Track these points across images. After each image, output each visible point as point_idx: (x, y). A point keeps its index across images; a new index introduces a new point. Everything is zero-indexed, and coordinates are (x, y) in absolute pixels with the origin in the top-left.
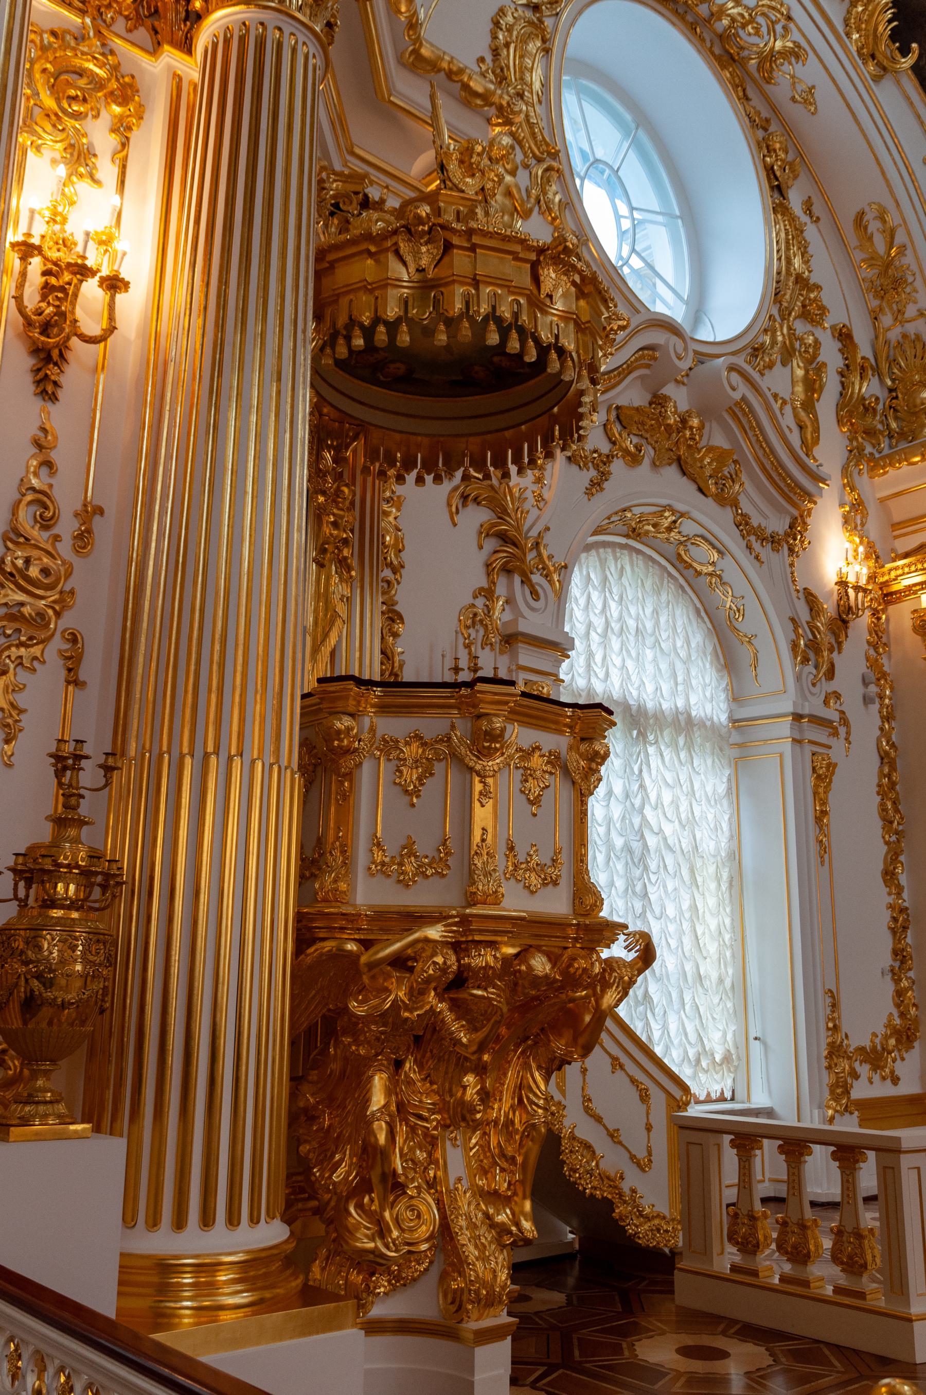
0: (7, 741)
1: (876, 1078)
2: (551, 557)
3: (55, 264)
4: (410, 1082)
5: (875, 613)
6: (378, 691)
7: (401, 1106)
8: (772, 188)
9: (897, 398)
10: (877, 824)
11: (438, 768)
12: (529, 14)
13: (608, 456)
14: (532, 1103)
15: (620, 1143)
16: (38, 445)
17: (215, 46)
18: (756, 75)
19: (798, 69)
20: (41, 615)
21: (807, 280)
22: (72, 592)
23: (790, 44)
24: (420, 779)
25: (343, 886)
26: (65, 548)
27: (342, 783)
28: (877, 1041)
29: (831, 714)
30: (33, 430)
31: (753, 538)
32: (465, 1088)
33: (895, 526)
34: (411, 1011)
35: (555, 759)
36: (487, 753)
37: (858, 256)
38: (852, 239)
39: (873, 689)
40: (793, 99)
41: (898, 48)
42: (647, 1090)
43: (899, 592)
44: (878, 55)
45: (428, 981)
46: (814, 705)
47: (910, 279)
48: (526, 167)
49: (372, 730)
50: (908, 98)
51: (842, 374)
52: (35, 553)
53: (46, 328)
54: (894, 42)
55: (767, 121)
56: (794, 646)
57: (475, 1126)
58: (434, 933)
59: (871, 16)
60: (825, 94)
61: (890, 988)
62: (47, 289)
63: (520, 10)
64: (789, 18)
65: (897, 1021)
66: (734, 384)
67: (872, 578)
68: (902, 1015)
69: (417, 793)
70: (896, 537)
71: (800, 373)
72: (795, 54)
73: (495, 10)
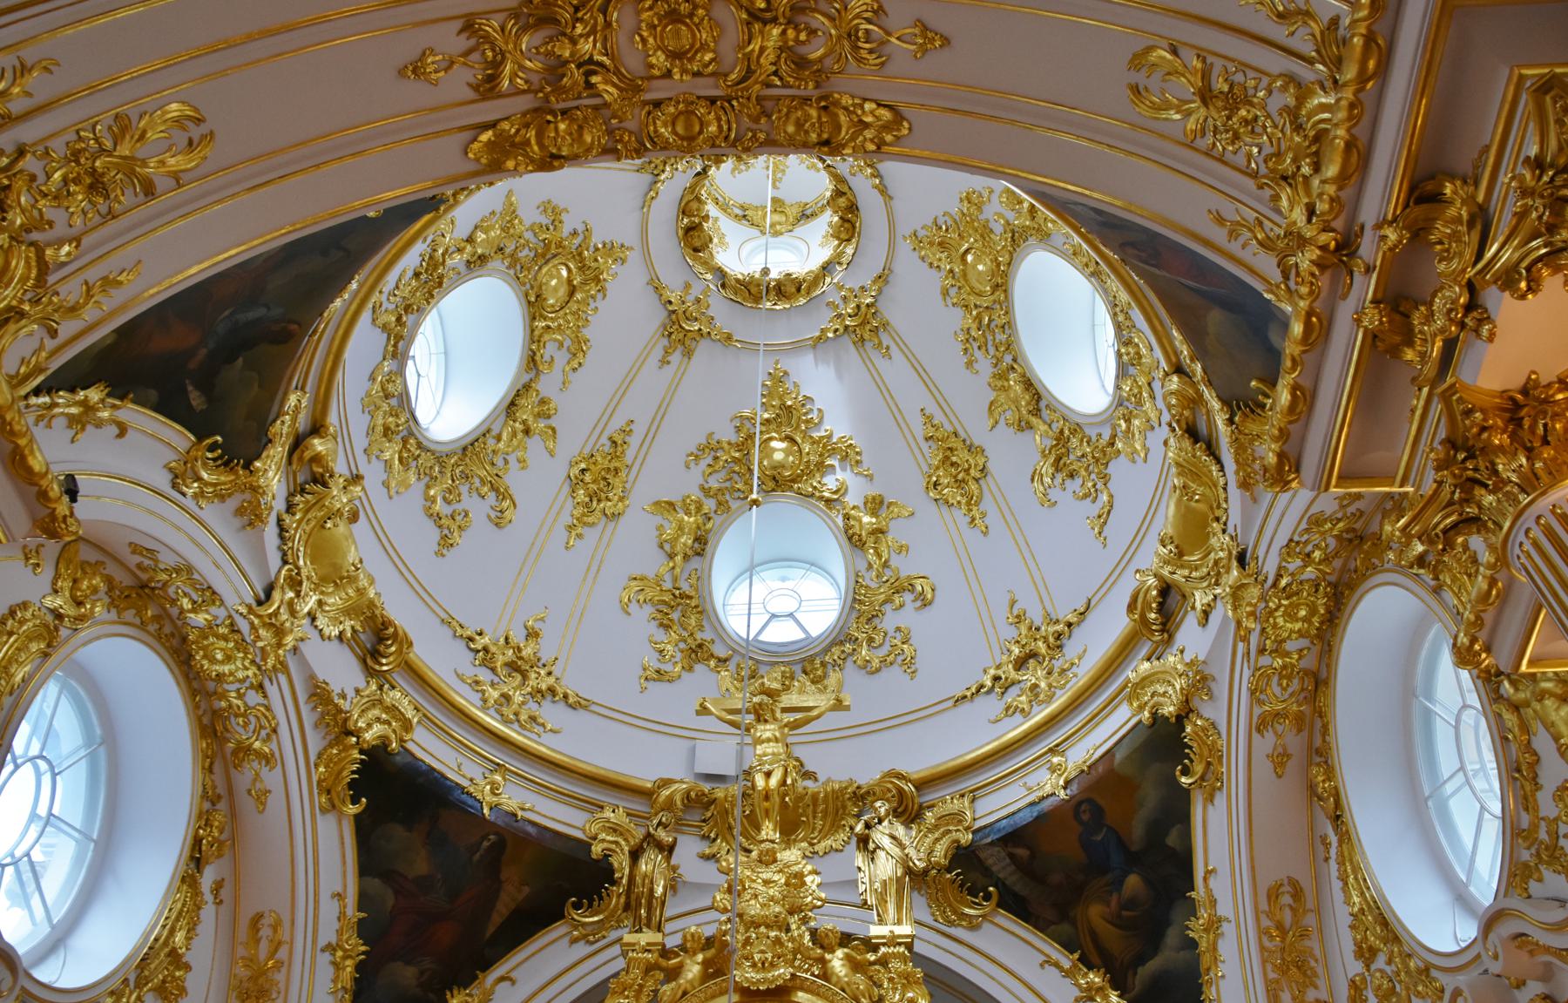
8: (192, 858)
12: (49, 618)
18: (229, 756)
19: (265, 771)
21: (180, 956)
23: (267, 750)
37: (241, 951)
40: (249, 792)
41: (351, 796)
44: (333, 793)
47: (274, 996)
50: (342, 838)
54: (350, 789)
55: (219, 797)
59: (340, 760)
60: (275, 801)
63: (44, 610)
64: (275, 731)
72: (267, 759)
73: (19, 601)
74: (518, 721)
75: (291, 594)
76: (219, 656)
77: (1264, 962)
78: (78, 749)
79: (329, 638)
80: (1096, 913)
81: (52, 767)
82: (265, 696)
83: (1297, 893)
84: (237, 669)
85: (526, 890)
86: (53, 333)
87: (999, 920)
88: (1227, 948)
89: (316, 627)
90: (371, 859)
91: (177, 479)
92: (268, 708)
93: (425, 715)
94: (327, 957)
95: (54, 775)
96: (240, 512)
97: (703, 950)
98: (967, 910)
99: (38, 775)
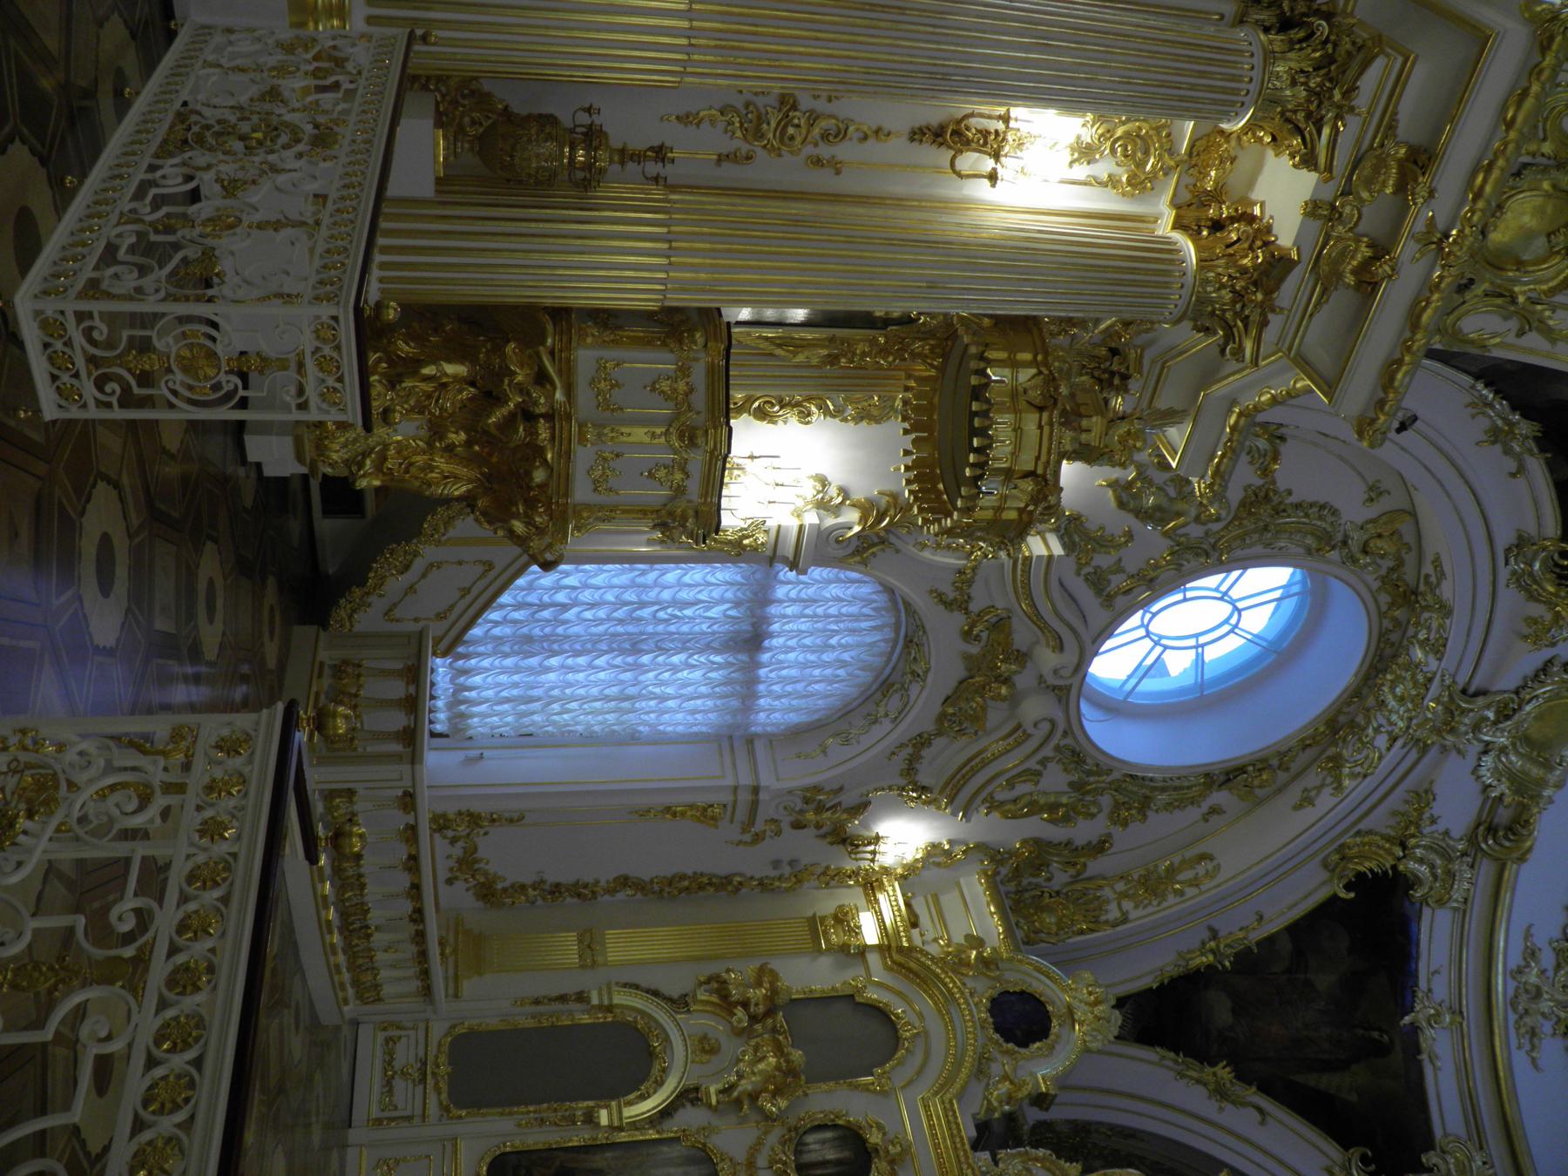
0: (678, 118)
1: (452, 863)
2: (874, 554)
3: (1004, 139)
4: (460, 391)
5: (855, 874)
6: (723, 363)
7: (444, 385)
8: (1227, 774)
9: (1051, 896)
10: (668, 871)
11: (672, 404)
12: (1339, 537)
13: (966, 609)
14: (446, 485)
15: (406, 594)
16: (878, 131)
17: (1169, 243)
20: (762, 136)
22: (780, 155)
24: (663, 392)
25: (589, 340)
26: (809, 150)
27: (659, 339)
28: (482, 865)
29: (759, 826)
30: (887, 126)
31: (910, 750)
32: (457, 433)
33: (936, 898)
34: (509, 385)
35: (680, 491)
36: (681, 437)
38: (1190, 853)
39: (787, 870)
42: (445, 618)
43: (875, 896)
45: (529, 394)
46: (766, 811)
48: (1207, 533)
49: (696, 360)
51: (1068, 843)
52: (804, 131)
53: (956, 133)
55: (1288, 769)
56: (817, 789)
57: (430, 444)
58: (559, 395)
61: (527, 879)
62: (985, 133)
64: (1365, 776)
65: (499, 886)
66: (1040, 726)
67: (886, 871)
68: (505, 890)
69: (653, 389)
71: (1064, 800)
73: (1337, 506)
74: (1521, 1017)
75: (1491, 715)
76: (1398, 691)
78: (1266, 640)
79: (1479, 777)
81: (1236, 626)
82: (1389, 749)
84: (1397, 712)
85: (1354, 1098)
86: (1521, 333)
89: (1480, 759)
90: (1305, 930)
91: (1521, 544)
92: (1380, 758)
93: (1465, 911)
94: (1206, 934)
95: (1232, 631)
96: (1532, 621)
99: (1226, 621)
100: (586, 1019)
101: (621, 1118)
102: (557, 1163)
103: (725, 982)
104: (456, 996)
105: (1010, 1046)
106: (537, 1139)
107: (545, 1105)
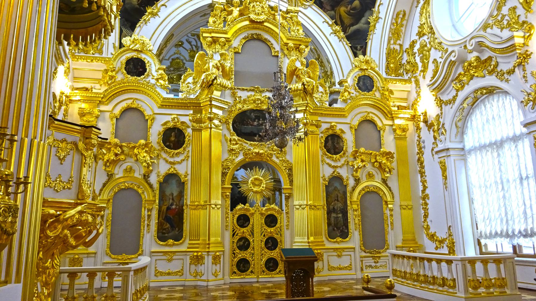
70: (74, 82)
77: (390, 32)
80: (342, 10)
83: (404, 15)
87: (313, 7)
88: (379, 26)
97: (239, 6)
98: (304, 3)
100: (111, 209)
101: (152, 201)
102: (163, 221)
103: (108, 160)
104: (95, 253)
105: (146, 74)
106: (154, 227)
107: (142, 223)
